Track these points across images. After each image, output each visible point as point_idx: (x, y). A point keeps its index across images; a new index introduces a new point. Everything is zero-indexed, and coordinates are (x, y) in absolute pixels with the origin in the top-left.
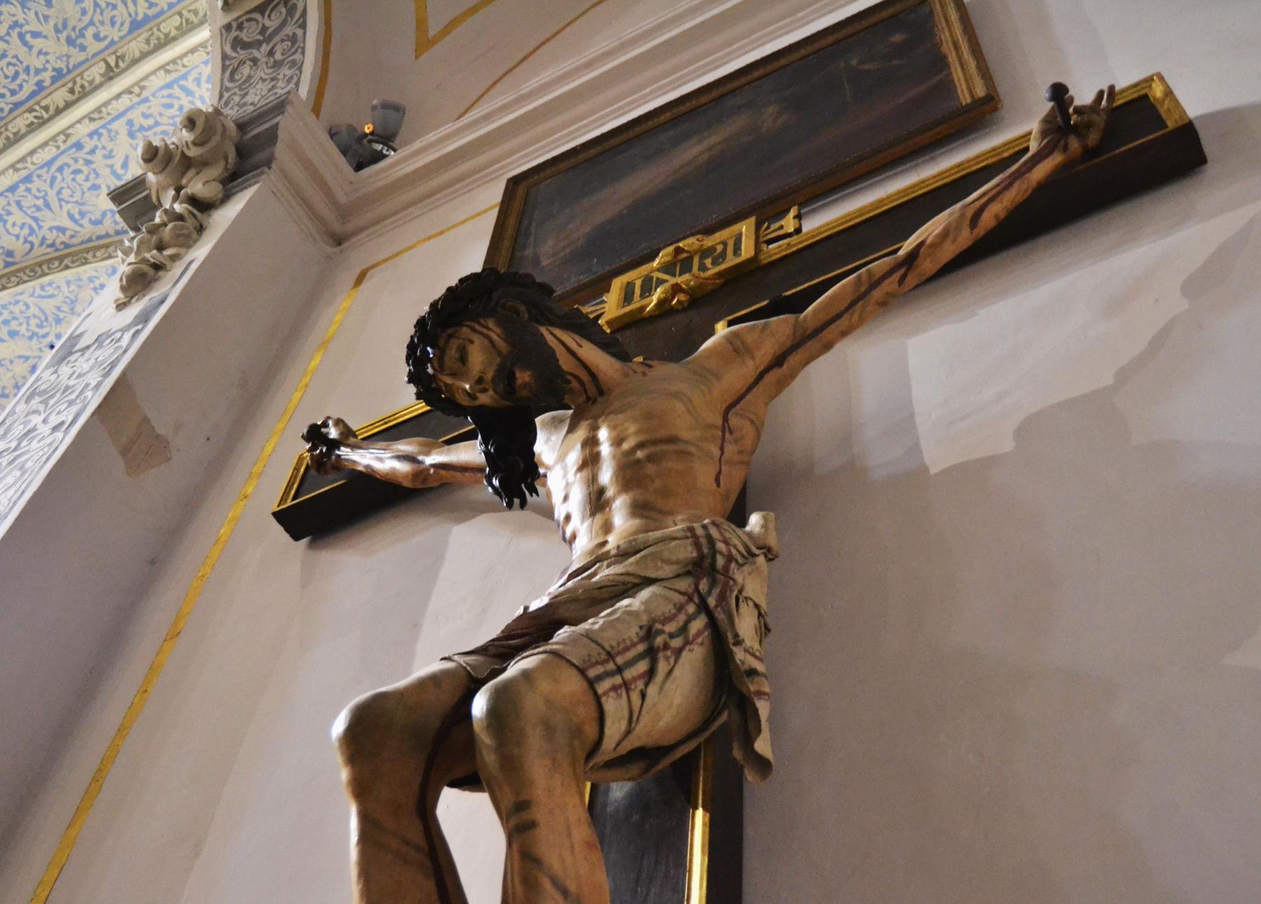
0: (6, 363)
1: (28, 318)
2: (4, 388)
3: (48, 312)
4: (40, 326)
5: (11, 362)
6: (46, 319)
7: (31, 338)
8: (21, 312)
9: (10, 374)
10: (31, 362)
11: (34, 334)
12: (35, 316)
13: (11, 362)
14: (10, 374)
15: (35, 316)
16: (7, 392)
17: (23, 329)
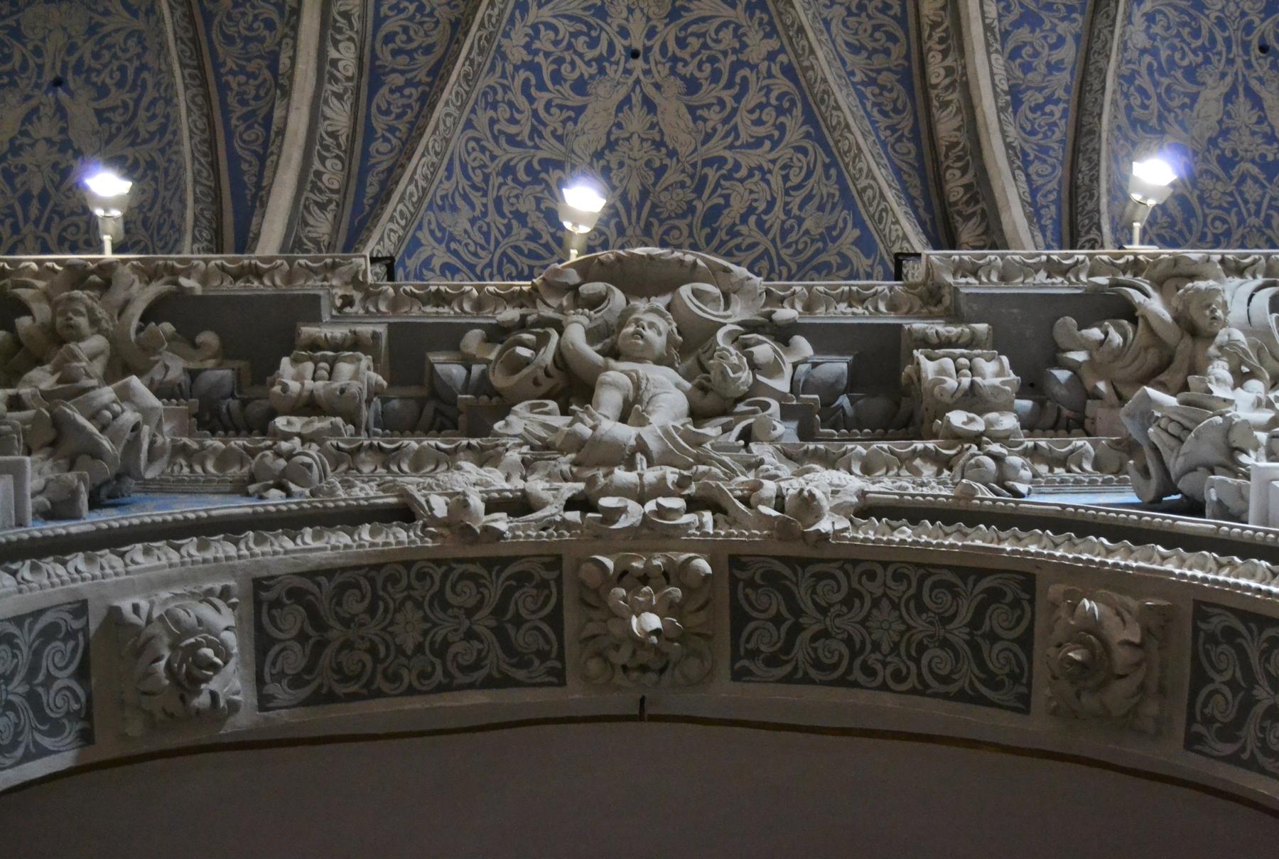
0: (616, 133)
1: (570, 46)
2: (648, 163)
3: (579, 12)
4: (593, 43)
5: (619, 126)
6: (590, 27)
7: (602, 71)
8: (556, 43)
9: (635, 141)
10: (636, 98)
11: (599, 60)
12: (575, 35)
13: (619, 126)
14: (635, 141)
15: (575, 35)
16: (657, 164)
17: (587, 71)
